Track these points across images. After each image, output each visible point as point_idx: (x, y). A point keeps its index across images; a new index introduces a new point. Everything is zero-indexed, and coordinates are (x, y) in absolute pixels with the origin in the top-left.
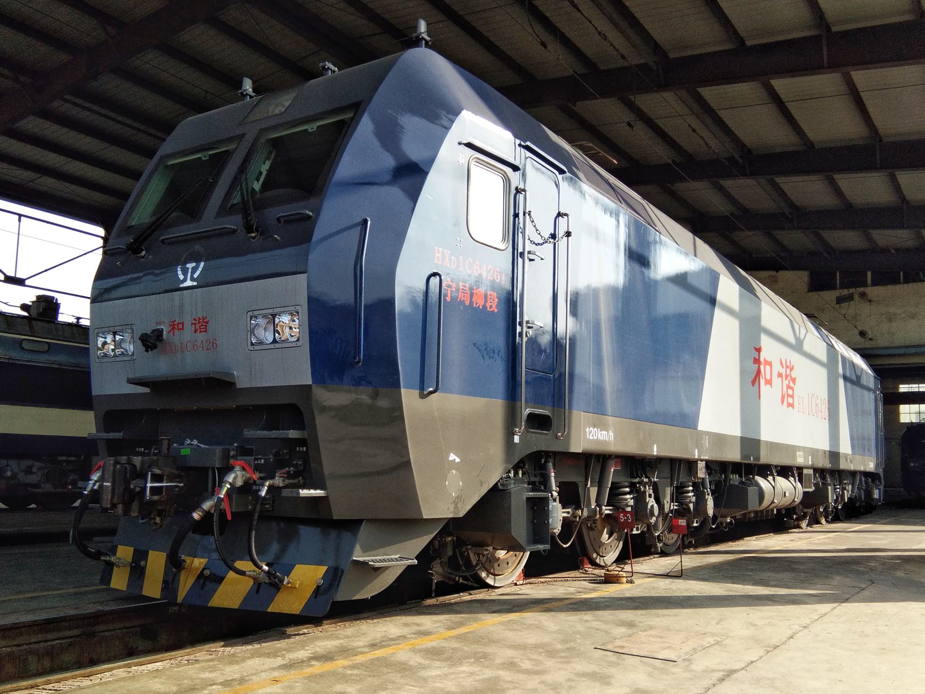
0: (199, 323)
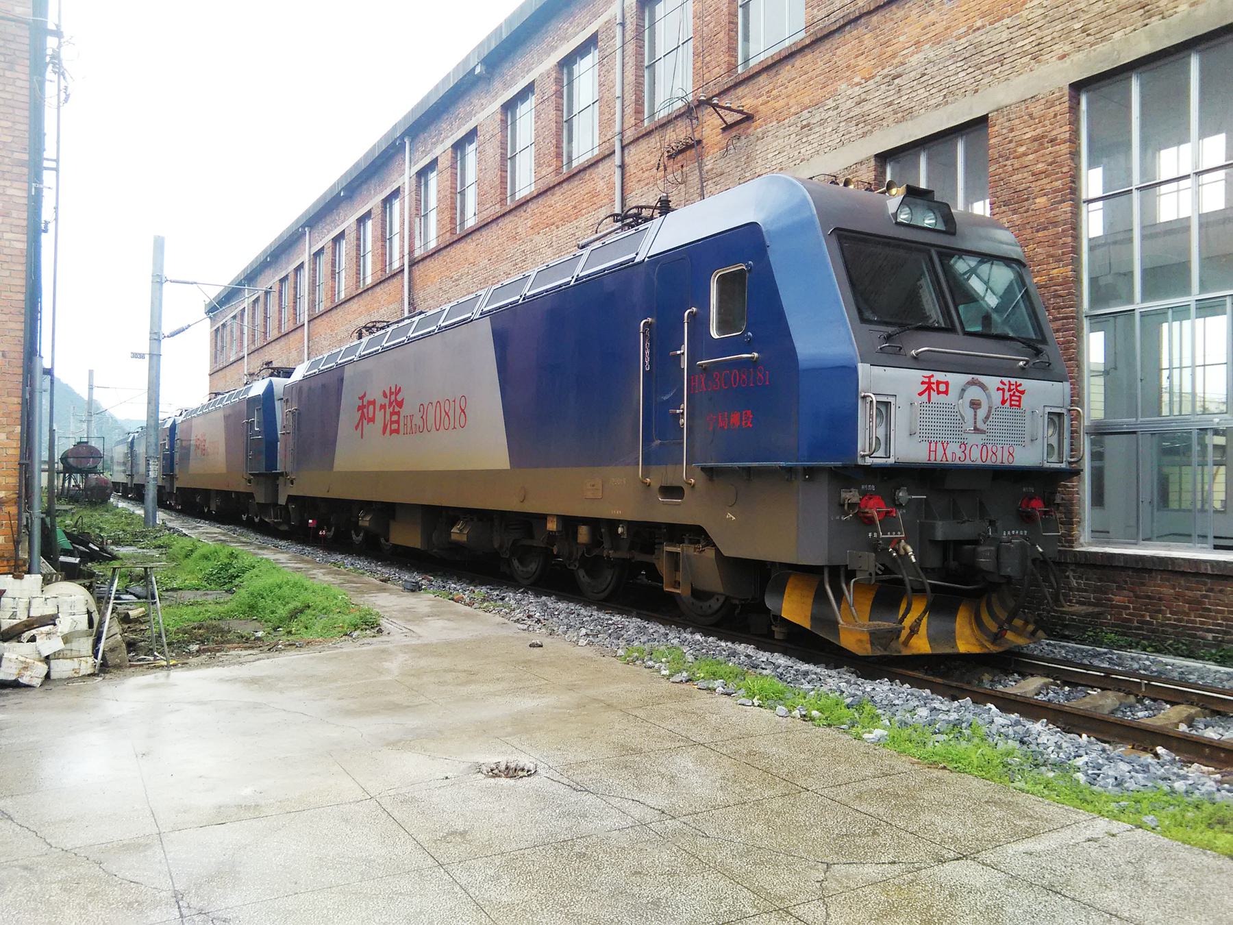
0: (1010, 390)
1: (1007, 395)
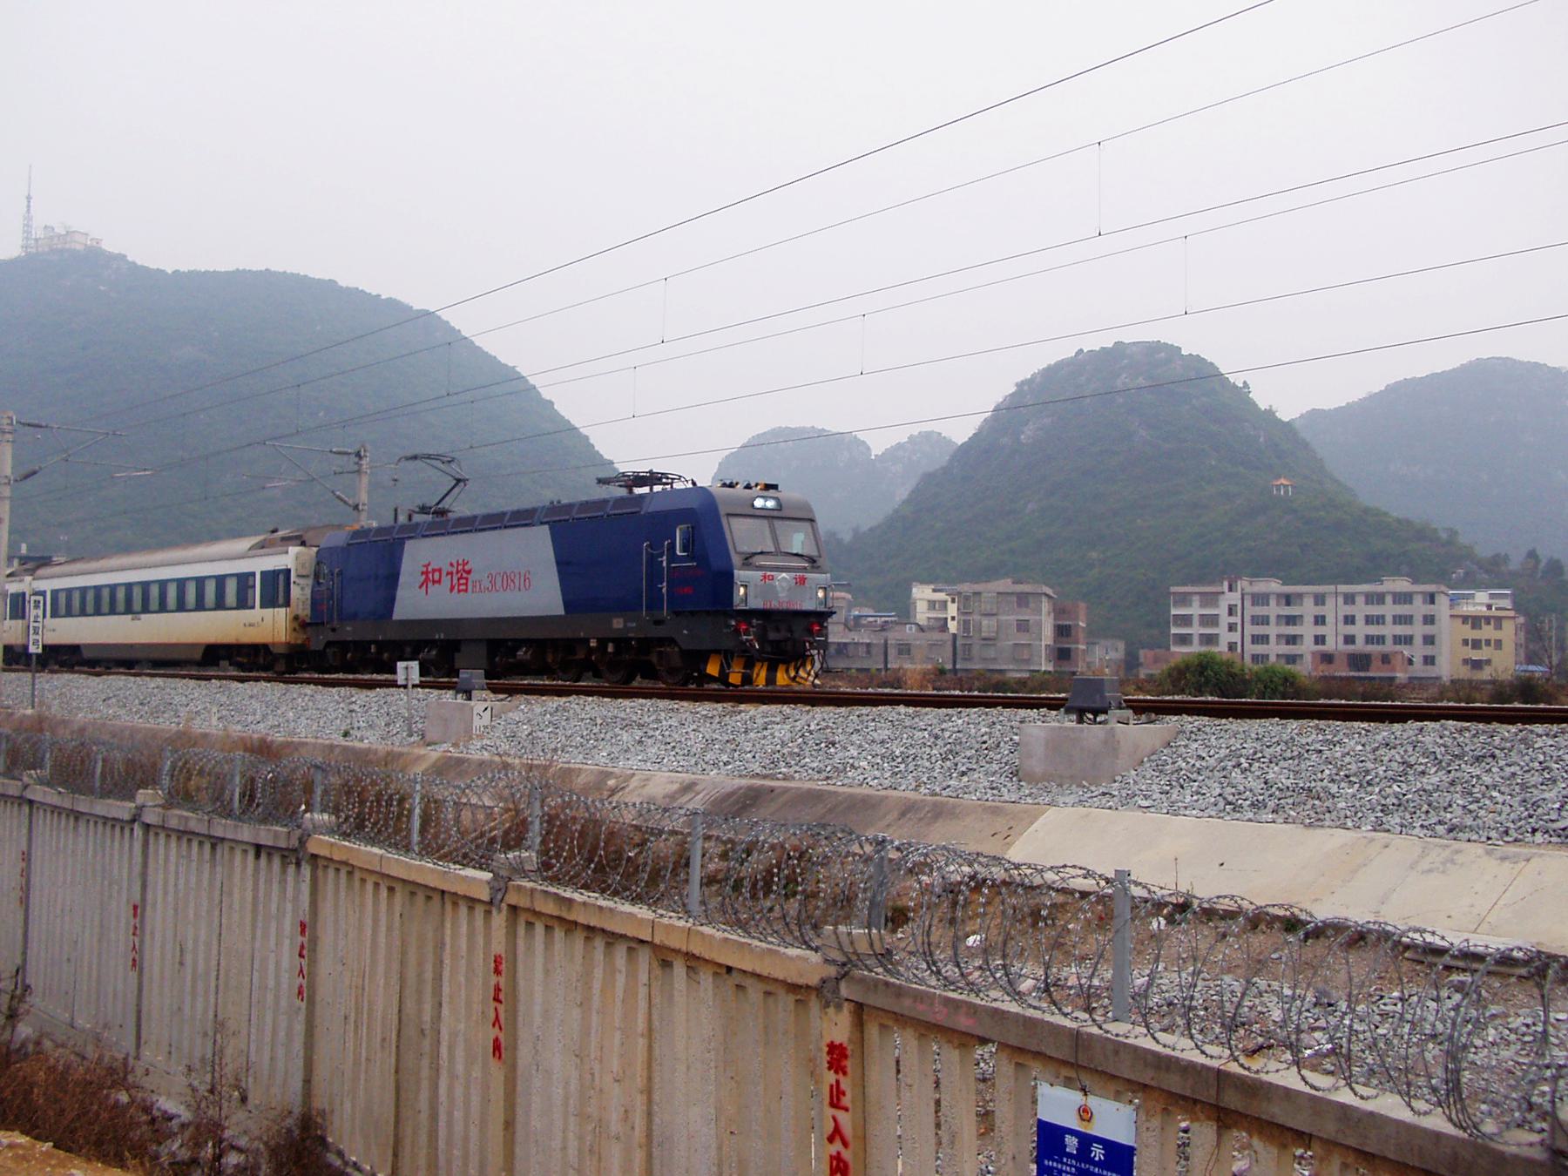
0: (458, 572)
1: (455, 581)
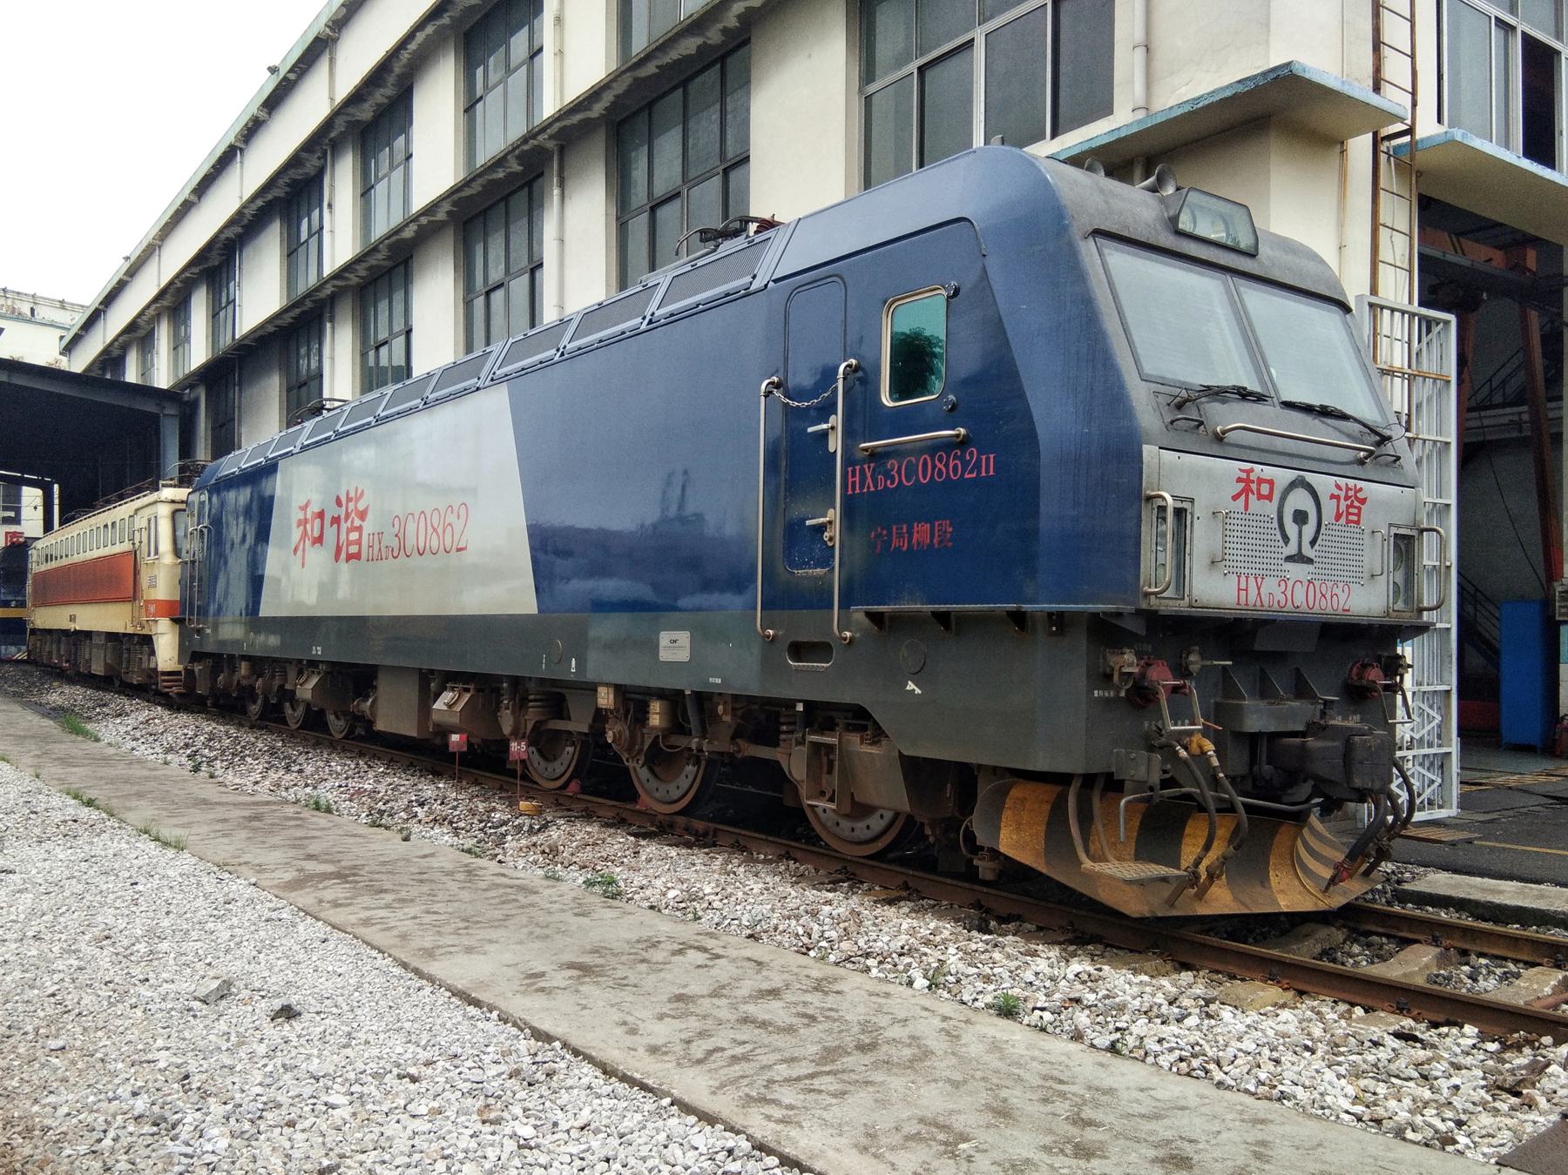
0: (1347, 498)
